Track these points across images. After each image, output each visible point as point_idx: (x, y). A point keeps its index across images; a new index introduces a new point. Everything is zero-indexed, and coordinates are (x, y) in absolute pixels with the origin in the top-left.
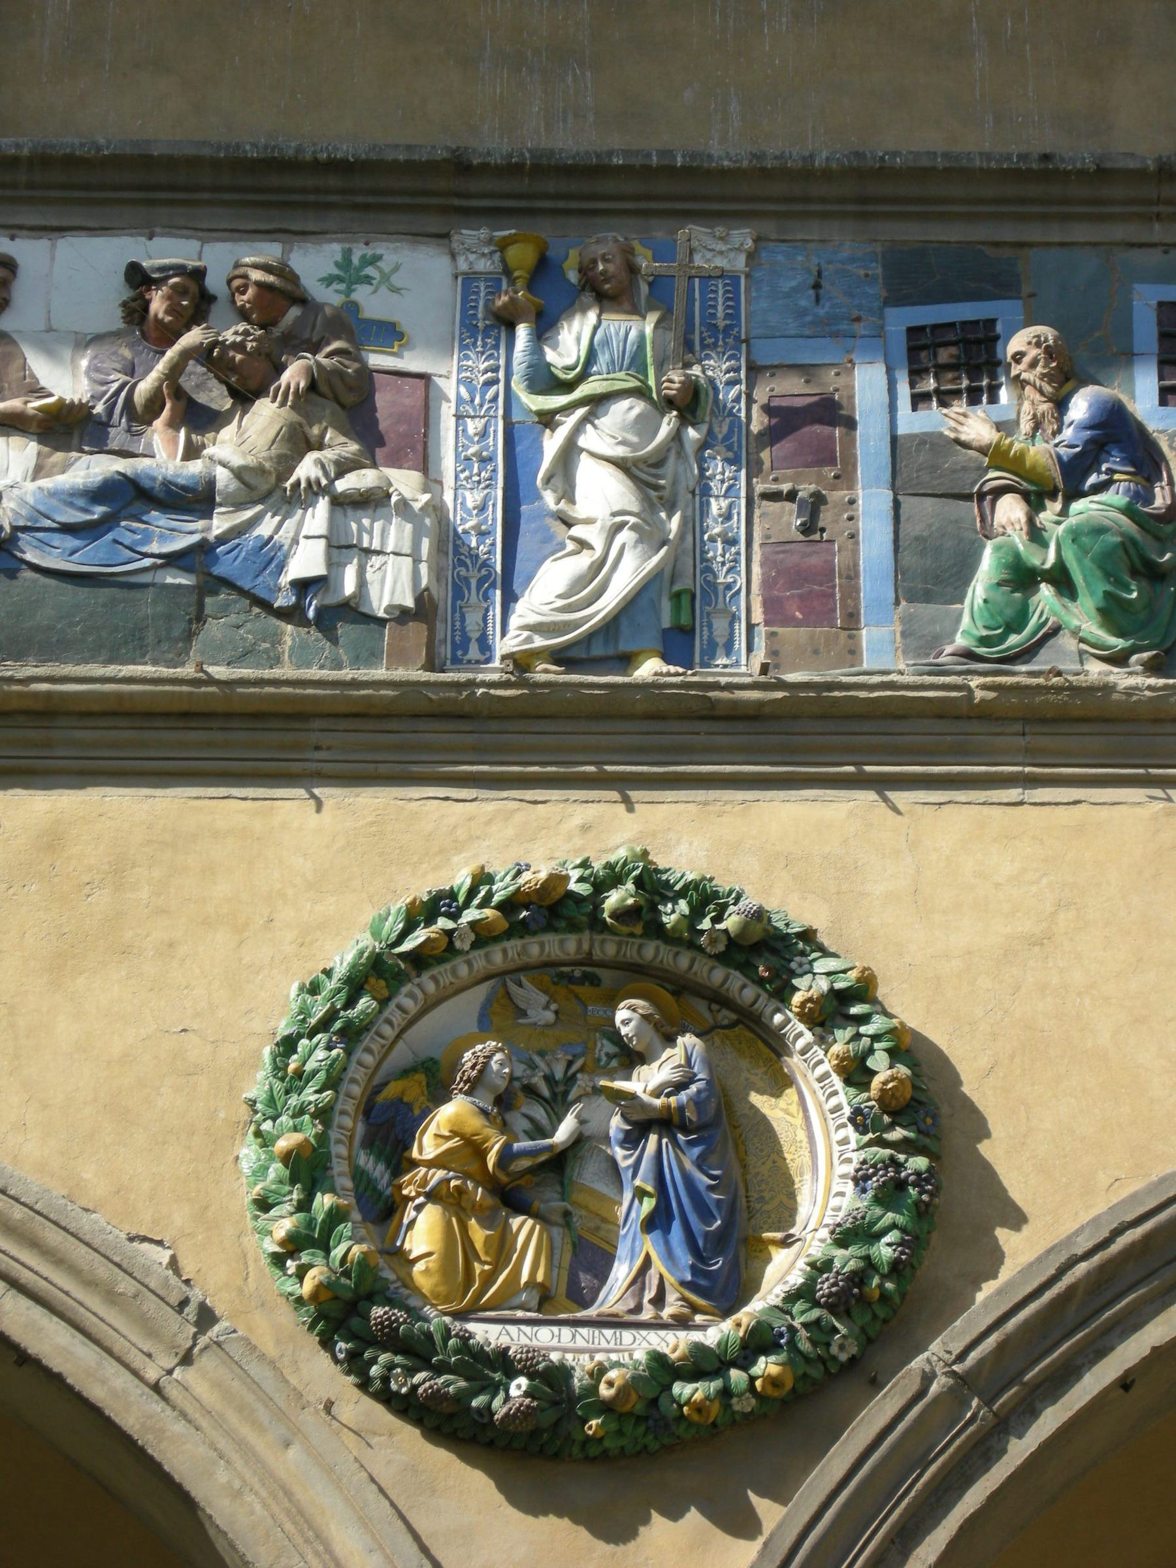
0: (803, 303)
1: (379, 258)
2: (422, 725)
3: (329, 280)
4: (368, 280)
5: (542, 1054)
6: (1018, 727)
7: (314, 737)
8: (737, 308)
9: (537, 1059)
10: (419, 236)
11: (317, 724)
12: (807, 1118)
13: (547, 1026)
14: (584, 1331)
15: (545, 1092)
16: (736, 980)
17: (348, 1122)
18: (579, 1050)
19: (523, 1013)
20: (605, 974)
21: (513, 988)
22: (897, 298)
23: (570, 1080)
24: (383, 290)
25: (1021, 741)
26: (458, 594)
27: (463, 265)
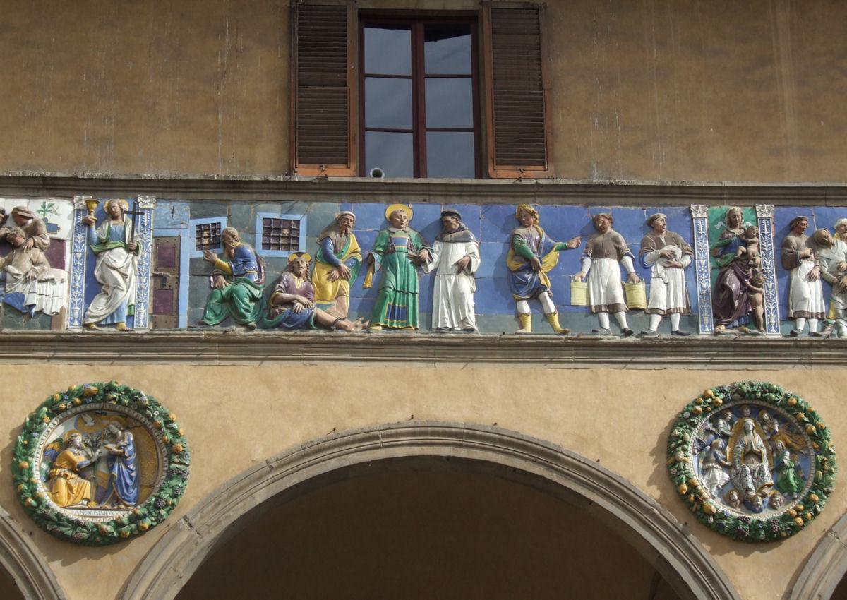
0: (168, 218)
1: (53, 204)
2: (61, 344)
3: (39, 212)
4: (50, 211)
5: (90, 434)
6: (217, 345)
7: (33, 347)
8: (150, 220)
9: (89, 436)
10: (64, 197)
11: (33, 344)
12: (157, 454)
13: (92, 426)
14: (97, 511)
15: (91, 444)
16: (140, 416)
17: (39, 455)
18: (100, 433)
19: (86, 423)
20: (107, 412)
21: (83, 416)
22: (194, 217)
23: (97, 441)
24: (54, 215)
25: (217, 348)
26: (72, 306)
27: (76, 207)
